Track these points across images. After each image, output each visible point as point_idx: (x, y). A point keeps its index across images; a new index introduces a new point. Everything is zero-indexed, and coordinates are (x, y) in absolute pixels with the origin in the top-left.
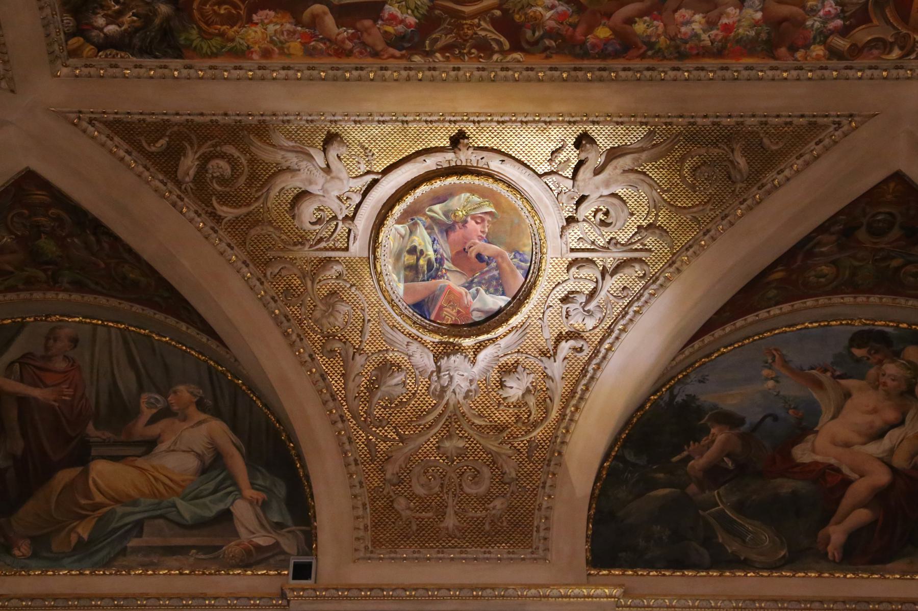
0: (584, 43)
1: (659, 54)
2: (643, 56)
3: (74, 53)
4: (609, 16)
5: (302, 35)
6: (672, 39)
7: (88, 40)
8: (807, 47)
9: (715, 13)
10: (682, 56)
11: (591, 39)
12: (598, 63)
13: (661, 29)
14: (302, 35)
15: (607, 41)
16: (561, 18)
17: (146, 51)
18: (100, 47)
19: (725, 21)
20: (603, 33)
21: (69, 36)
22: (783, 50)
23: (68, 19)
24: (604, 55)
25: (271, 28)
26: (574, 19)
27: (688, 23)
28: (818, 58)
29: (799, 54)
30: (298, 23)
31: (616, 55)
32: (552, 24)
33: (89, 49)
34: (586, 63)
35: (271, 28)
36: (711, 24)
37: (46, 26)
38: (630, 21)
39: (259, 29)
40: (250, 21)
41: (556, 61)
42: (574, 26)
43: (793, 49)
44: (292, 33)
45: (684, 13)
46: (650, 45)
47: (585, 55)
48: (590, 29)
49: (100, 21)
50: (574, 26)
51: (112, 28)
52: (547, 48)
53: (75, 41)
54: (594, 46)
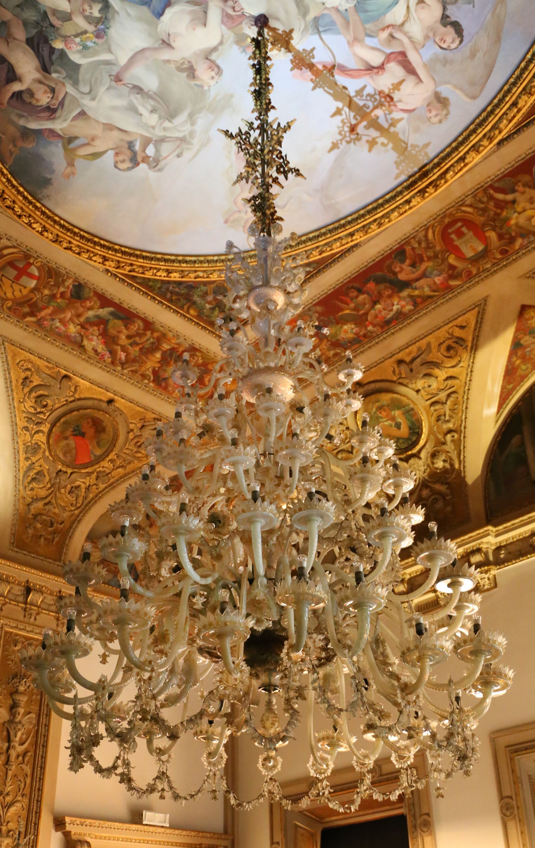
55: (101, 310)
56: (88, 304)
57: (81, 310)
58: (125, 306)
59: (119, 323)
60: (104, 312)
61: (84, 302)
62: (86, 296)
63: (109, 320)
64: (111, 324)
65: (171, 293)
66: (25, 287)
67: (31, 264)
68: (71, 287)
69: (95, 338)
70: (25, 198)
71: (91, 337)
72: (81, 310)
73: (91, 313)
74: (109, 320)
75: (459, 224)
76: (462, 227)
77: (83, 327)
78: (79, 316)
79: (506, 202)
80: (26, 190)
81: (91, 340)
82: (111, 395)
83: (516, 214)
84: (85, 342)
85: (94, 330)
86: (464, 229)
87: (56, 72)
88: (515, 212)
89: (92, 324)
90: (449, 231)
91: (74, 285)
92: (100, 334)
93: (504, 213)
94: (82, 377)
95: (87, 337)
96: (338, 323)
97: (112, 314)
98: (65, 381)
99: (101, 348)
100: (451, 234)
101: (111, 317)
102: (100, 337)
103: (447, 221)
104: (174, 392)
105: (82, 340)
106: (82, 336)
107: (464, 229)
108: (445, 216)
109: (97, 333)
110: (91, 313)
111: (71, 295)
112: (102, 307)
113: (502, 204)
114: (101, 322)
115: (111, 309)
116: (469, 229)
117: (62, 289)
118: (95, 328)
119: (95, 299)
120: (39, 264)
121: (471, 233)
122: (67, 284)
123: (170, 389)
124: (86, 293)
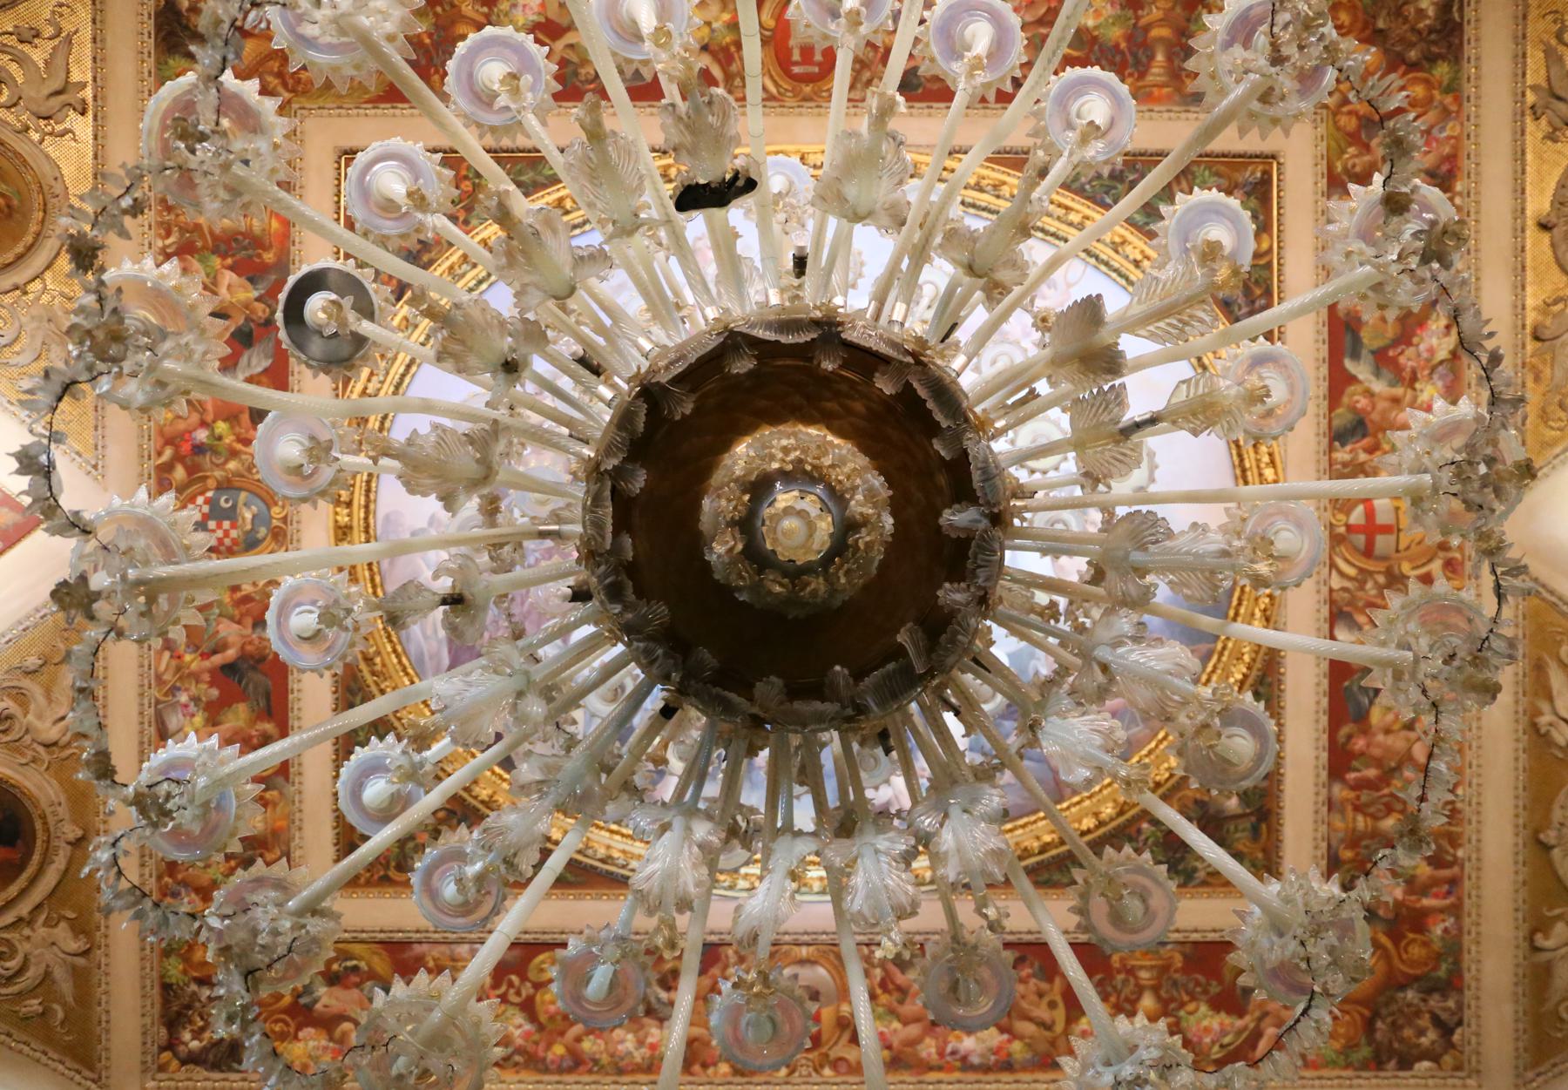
0: (544, 1059)
1: (602, 1070)
2: (590, 1072)
3: (162, 1068)
4: (562, 1034)
5: (334, 1051)
6: (612, 1056)
7: (176, 1055)
8: (715, 1064)
9: (641, 1034)
10: (621, 1072)
11: (550, 1056)
12: (556, 1078)
13: (603, 1047)
14: (334, 1051)
15: (562, 1057)
16: (527, 1035)
17: (216, 1066)
18: (184, 1063)
19: (650, 1040)
20: (559, 1050)
21: (163, 1049)
22: (697, 1068)
23: (164, 1032)
24: (560, 1070)
25: (311, 1044)
26: (536, 1037)
27: (622, 1041)
28: (725, 1075)
29: (711, 1071)
30: (331, 1039)
31: (570, 1070)
32: (519, 1042)
33: (175, 1063)
34: (546, 1078)
35: (311, 1044)
36: (640, 1043)
37: (144, 1034)
38: (578, 1040)
39: (301, 1045)
40: (296, 1038)
41: (524, 1075)
42: (536, 1043)
43: (705, 1066)
44: (325, 1048)
45: (618, 1033)
46: (596, 1061)
47: (547, 1071)
48: (549, 1046)
49: (187, 1036)
50: (536, 1043)
51: (195, 1044)
52: (516, 1064)
53: (167, 1055)
54: (553, 1062)
55: (1361, 377)
56: (1363, 402)
57: (1382, 405)
58: (1324, 351)
59: (1365, 335)
60: (1360, 370)
61: (1363, 410)
62: (1350, 416)
63: (1373, 352)
64: (1376, 344)
65: (1253, 302)
66: (1397, 509)
67: (1349, 528)
68: (1348, 448)
69: (1422, 347)
70: (1240, 604)
71: (1425, 355)
72: (1382, 405)
73: (1379, 387)
74: (1373, 352)
75: (796, 70)
76: (796, 64)
77: (1414, 378)
78: (1396, 401)
79: (714, 55)
80: (1229, 607)
81: (1431, 351)
82: (1531, 232)
83: (715, 25)
84: (1442, 354)
85: (1408, 359)
86: (796, 56)
87: (1037, 673)
88: (713, 31)
89: (1397, 369)
90: (816, 69)
91: (1343, 445)
92: (1409, 344)
93: (728, 39)
94: (1519, 308)
95: (1428, 360)
96: (1095, 39)
97: (1356, 356)
98: (1547, 334)
99: (1438, 323)
100: (820, 64)
101: (1364, 352)
102: (1415, 340)
103: (807, 89)
104: (1449, 138)
105: (1441, 362)
106: (1433, 369)
107: (796, 56)
108: (805, 99)
109: (1410, 351)
110: (1379, 387)
111: (1364, 436)
112: (1353, 379)
113: (721, 56)
114: (1383, 360)
115: (1349, 364)
116: (789, 51)
117: (1363, 457)
118: (1402, 360)
119: (1345, 400)
120: (1341, 517)
121: (792, 43)
122: (1347, 457)
123: (1447, 150)
124: (1343, 417)
